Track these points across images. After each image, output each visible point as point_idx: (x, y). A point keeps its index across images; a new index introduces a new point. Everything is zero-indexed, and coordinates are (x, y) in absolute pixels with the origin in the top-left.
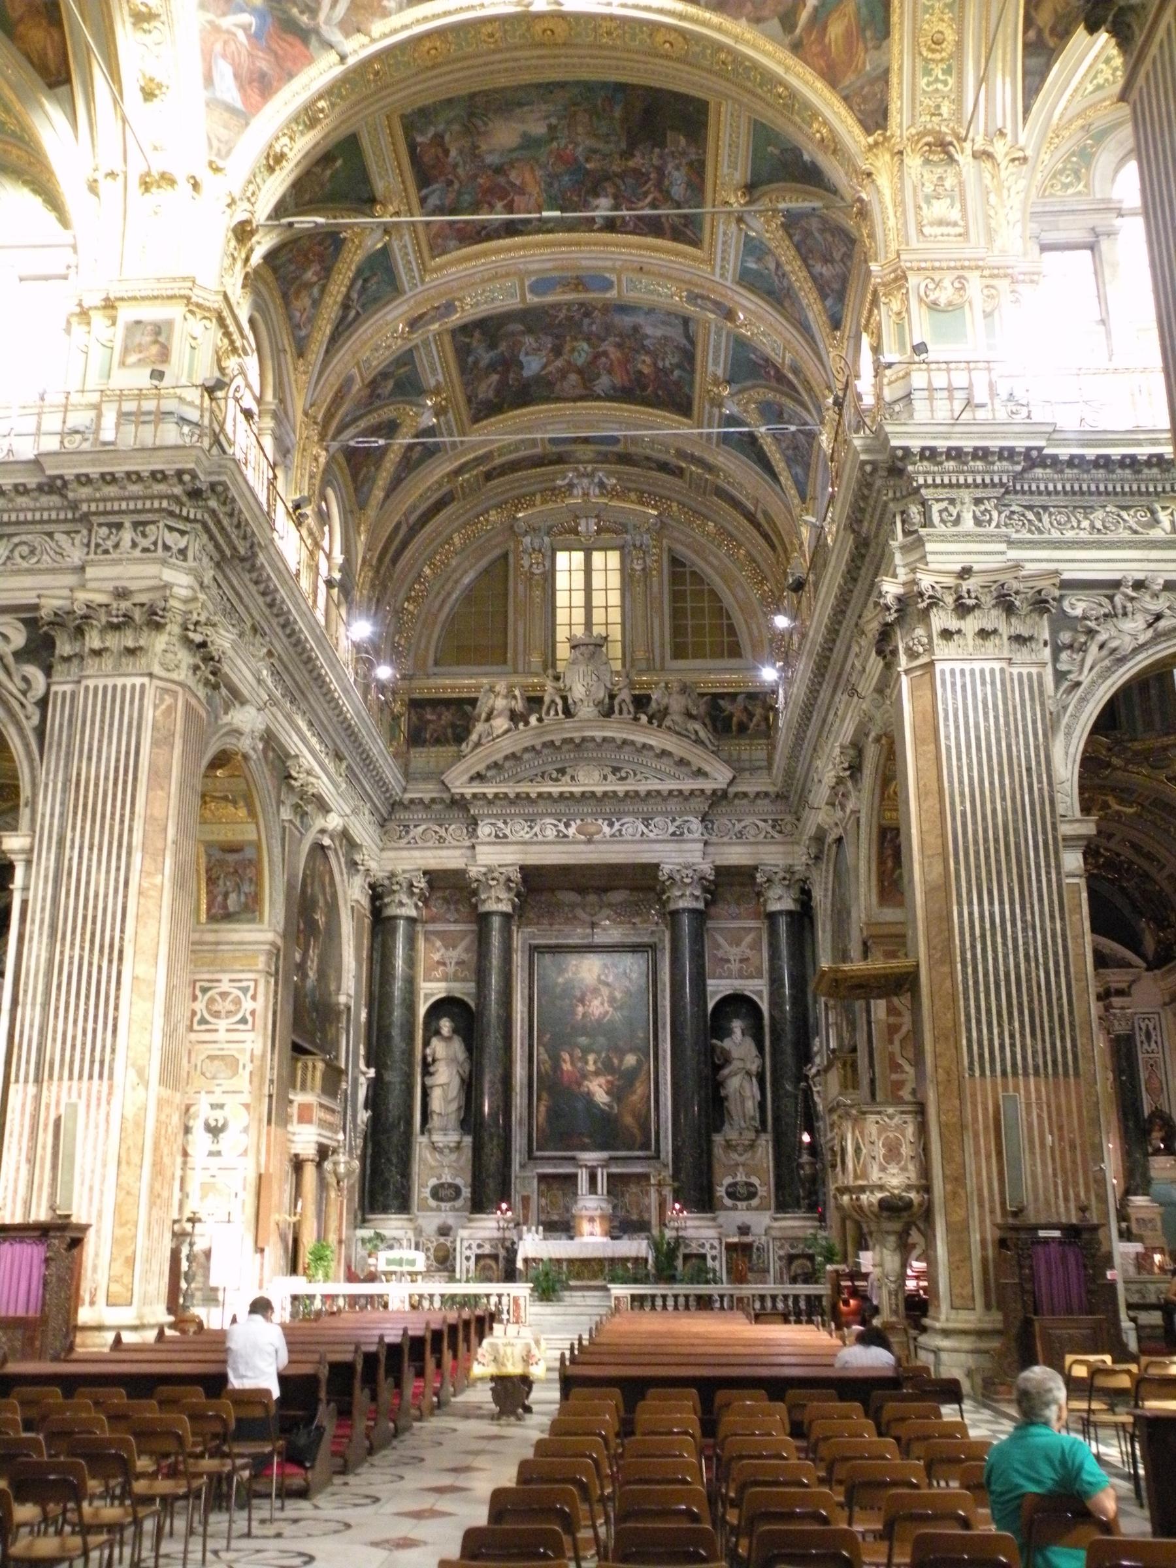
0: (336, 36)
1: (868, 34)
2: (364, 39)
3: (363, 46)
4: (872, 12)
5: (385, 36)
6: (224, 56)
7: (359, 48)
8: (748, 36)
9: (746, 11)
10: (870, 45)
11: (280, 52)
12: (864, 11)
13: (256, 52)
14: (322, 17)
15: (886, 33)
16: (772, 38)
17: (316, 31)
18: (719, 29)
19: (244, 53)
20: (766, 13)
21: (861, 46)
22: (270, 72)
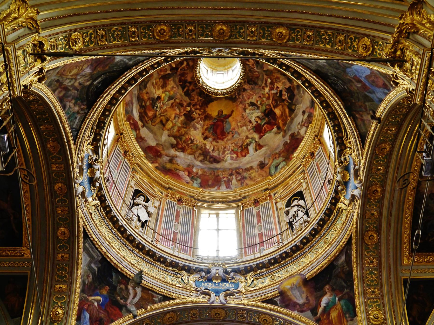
0: (133, 309)
1: (347, 316)
2: (143, 310)
3: (144, 313)
4: (348, 308)
5: (153, 310)
6: (87, 310)
7: (141, 313)
8: (298, 317)
9: (297, 308)
10: (348, 319)
11: (110, 312)
12: (344, 307)
13: (100, 310)
14: (129, 301)
15: (355, 314)
16: (309, 318)
17: (126, 306)
18: (286, 315)
19: (95, 310)
20: (305, 308)
21: (345, 320)
22: (105, 319)
